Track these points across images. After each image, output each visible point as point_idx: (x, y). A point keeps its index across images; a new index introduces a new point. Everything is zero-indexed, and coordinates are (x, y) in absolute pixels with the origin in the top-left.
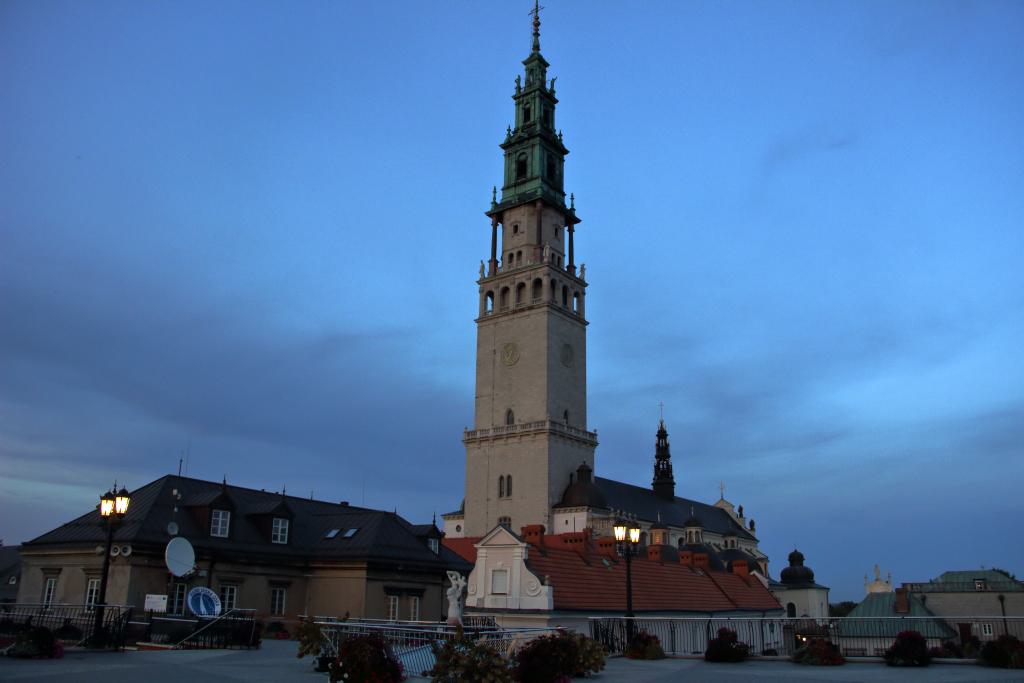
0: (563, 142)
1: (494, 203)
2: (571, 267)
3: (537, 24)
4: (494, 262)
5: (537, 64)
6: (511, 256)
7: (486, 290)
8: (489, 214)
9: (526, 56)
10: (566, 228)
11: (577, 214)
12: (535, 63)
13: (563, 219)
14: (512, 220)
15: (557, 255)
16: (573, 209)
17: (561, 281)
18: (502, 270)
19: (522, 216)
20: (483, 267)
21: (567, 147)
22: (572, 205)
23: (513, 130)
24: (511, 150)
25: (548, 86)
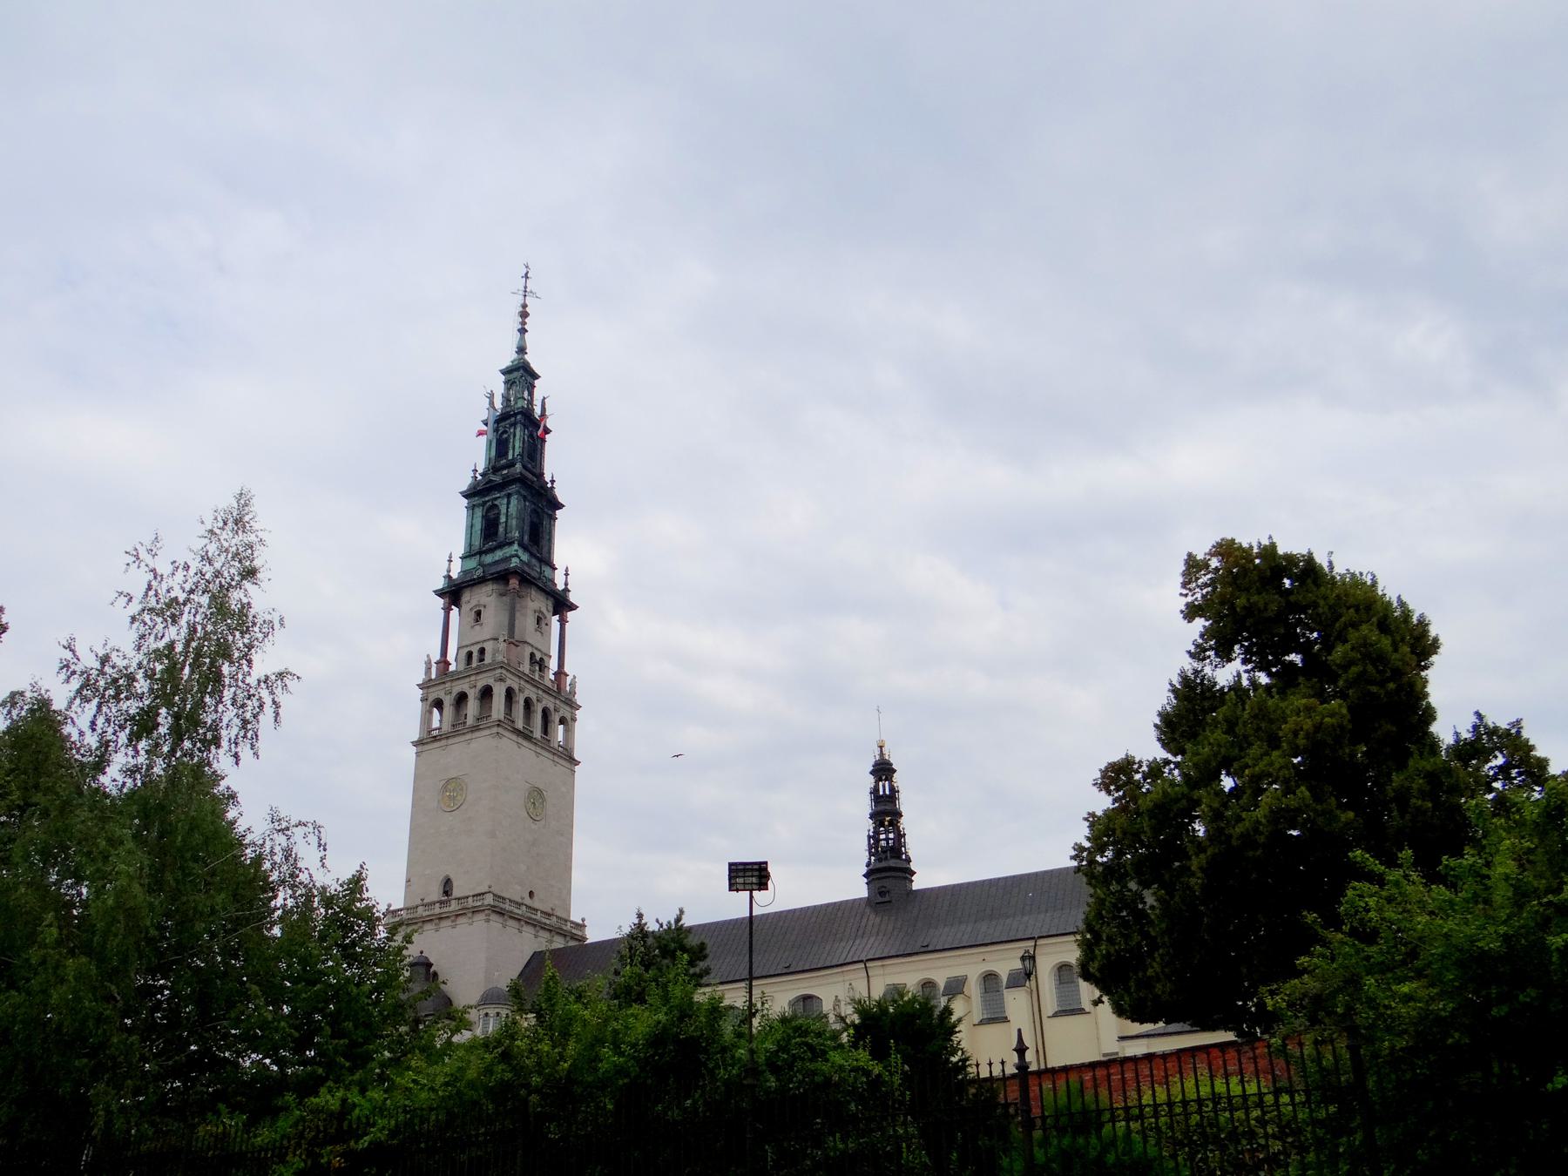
2: (560, 673)
3: (524, 315)
4: (443, 662)
5: (521, 374)
6: (470, 655)
8: (440, 593)
9: (506, 363)
11: (572, 598)
12: (516, 374)
14: (474, 602)
19: (486, 596)
23: (480, 470)
24: (477, 500)
25: (538, 411)
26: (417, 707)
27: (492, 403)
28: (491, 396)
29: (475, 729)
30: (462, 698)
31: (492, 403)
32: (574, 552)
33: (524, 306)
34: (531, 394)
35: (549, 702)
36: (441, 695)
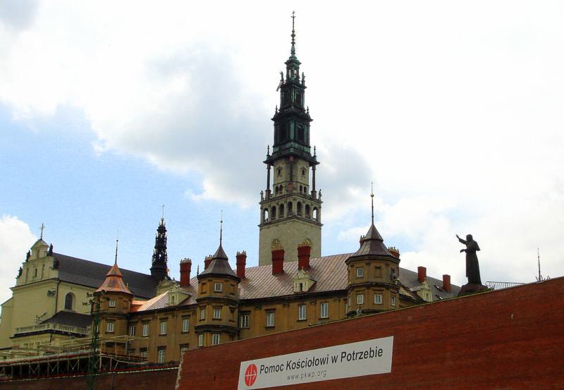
0: (310, 114)
1: (268, 155)
2: (314, 192)
3: (293, 36)
4: (268, 191)
5: (293, 64)
7: (264, 207)
10: (311, 168)
13: (308, 164)
14: (278, 166)
15: (303, 186)
16: (315, 156)
17: (304, 202)
18: (273, 196)
19: (282, 164)
20: (262, 194)
21: (312, 118)
22: (315, 154)
23: (279, 108)
25: (301, 79)
26: (259, 211)
27: (282, 77)
28: (282, 74)
29: (278, 221)
30: (274, 209)
31: (282, 77)
32: (319, 138)
33: (293, 31)
34: (298, 72)
35: (309, 202)
36: (267, 207)
